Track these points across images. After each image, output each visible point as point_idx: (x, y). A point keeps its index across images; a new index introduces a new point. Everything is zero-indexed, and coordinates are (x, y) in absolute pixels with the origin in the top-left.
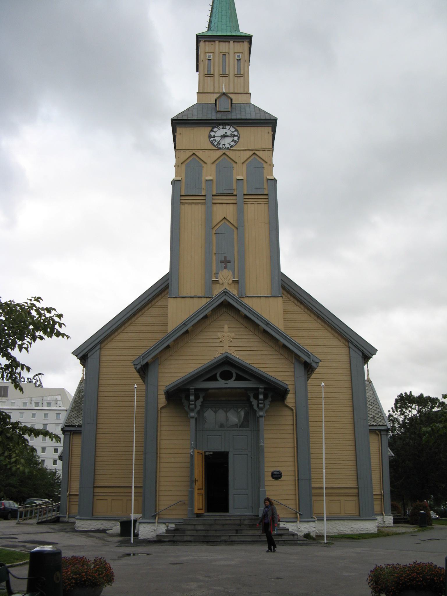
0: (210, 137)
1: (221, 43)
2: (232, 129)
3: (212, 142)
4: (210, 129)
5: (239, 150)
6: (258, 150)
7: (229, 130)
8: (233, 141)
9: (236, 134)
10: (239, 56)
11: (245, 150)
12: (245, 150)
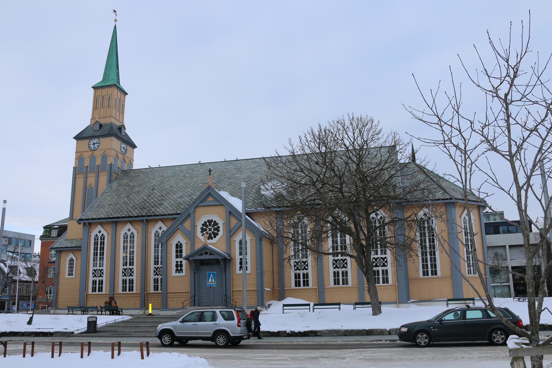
0: (89, 145)
1: (103, 89)
2: (98, 140)
3: (89, 147)
4: (89, 140)
5: (99, 150)
6: (107, 149)
7: (96, 141)
8: (97, 146)
9: (99, 142)
10: (110, 96)
11: (101, 150)
12: (101, 150)
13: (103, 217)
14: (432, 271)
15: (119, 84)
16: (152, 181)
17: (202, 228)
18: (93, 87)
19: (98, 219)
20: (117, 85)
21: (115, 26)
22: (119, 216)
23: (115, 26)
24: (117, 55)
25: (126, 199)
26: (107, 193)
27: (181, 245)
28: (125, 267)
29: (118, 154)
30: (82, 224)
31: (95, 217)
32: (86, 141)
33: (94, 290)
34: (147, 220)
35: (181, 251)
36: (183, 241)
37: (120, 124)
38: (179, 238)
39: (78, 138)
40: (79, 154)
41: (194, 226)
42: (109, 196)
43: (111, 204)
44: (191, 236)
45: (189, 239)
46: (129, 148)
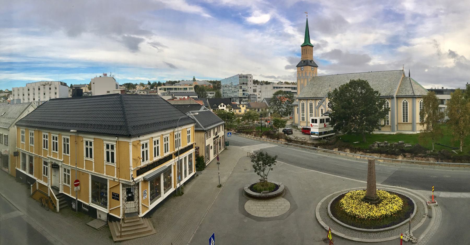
13: (303, 97)
14: (406, 121)
15: (310, 43)
16: (320, 82)
17: (328, 105)
18: (301, 46)
19: (302, 98)
20: (309, 44)
21: (307, 19)
22: (308, 97)
23: (307, 19)
24: (308, 31)
25: (311, 90)
26: (306, 87)
27: (322, 110)
28: (310, 114)
29: (311, 72)
30: (298, 99)
31: (301, 97)
32: (300, 68)
33: (302, 120)
34: (316, 99)
35: (322, 112)
36: (323, 108)
37: (311, 59)
38: (322, 107)
39: (297, 66)
40: (298, 72)
41: (326, 104)
42: (307, 88)
43: (306, 92)
44: (325, 107)
45: (324, 108)
46: (315, 68)
